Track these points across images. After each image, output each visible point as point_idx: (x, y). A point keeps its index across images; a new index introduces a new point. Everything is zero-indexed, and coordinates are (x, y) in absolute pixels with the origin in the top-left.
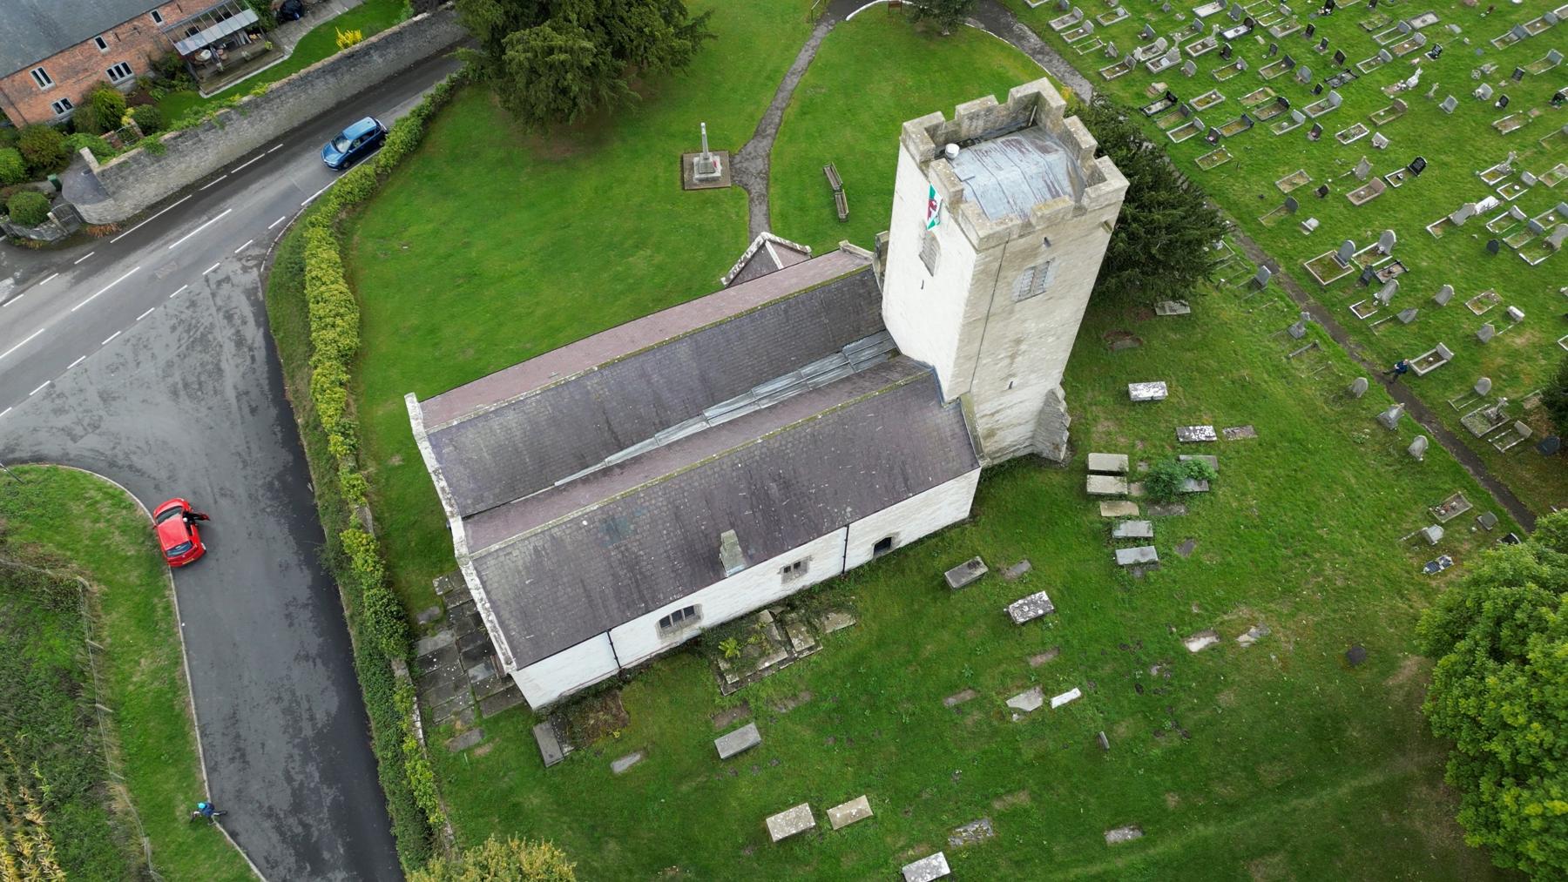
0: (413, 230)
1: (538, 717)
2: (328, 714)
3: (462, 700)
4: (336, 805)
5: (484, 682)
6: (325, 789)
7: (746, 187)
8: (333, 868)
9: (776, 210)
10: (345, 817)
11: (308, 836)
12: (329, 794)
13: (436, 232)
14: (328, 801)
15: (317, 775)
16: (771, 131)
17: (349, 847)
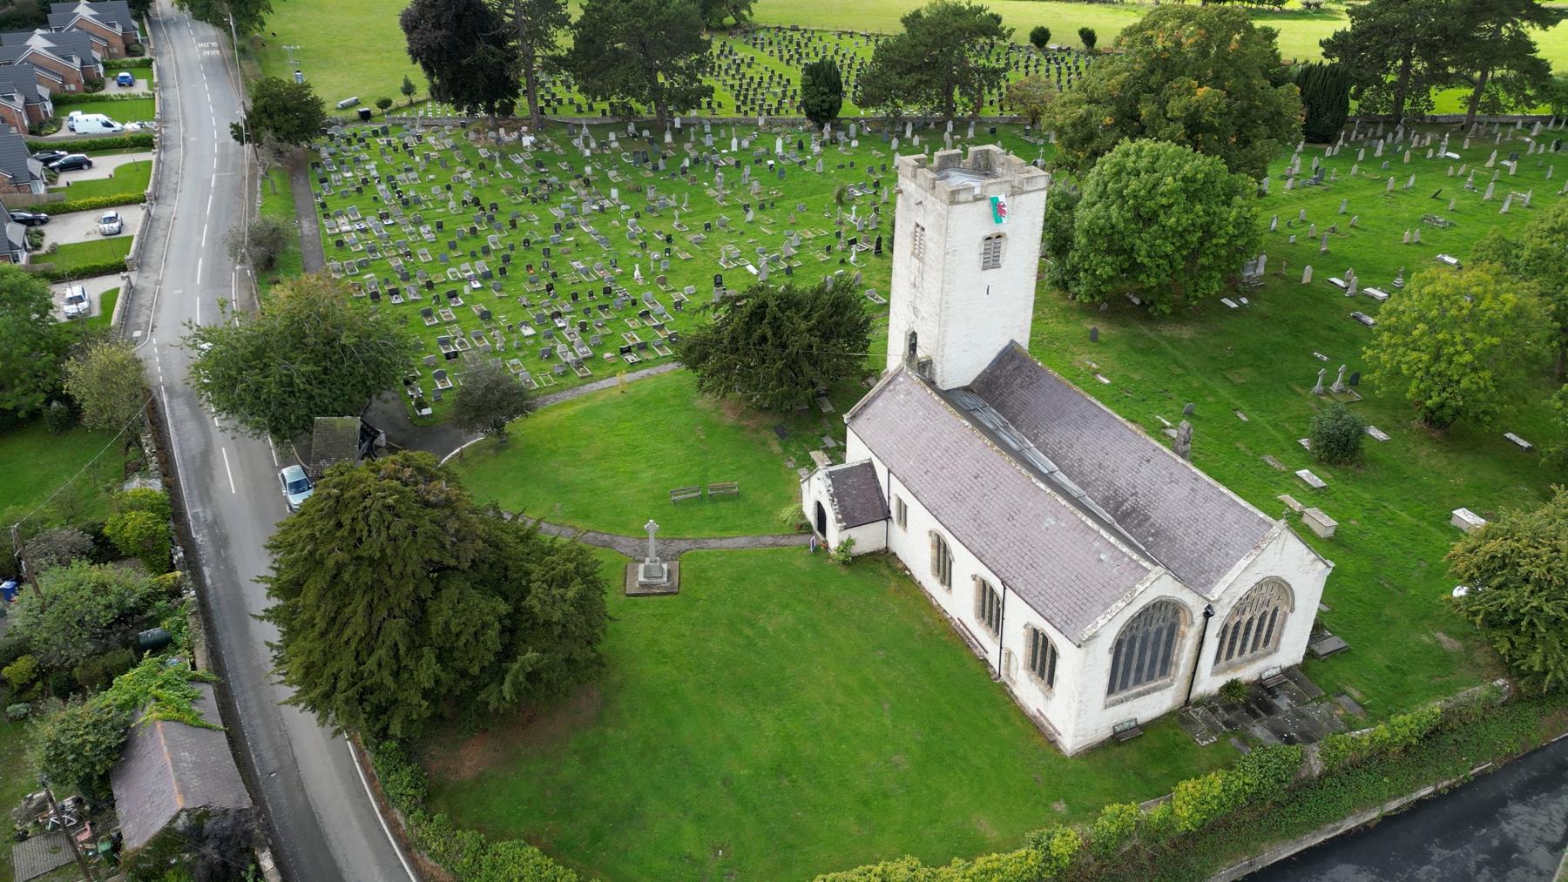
0: (689, 846)
1: (1310, 654)
2: (1359, 872)
3: (1317, 712)
4: (1448, 844)
5: (1291, 697)
6: (1435, 857)
7: (680, 553)
8: (1503, 835)
9: (717, 534)
10: (1453, 833)
11: (1488, 863)
12: (1439, 853)
13: (700, 818)
14: (1446, 853)
15: (1426, 868)
16: (606, 537)
17: (1478, 826)
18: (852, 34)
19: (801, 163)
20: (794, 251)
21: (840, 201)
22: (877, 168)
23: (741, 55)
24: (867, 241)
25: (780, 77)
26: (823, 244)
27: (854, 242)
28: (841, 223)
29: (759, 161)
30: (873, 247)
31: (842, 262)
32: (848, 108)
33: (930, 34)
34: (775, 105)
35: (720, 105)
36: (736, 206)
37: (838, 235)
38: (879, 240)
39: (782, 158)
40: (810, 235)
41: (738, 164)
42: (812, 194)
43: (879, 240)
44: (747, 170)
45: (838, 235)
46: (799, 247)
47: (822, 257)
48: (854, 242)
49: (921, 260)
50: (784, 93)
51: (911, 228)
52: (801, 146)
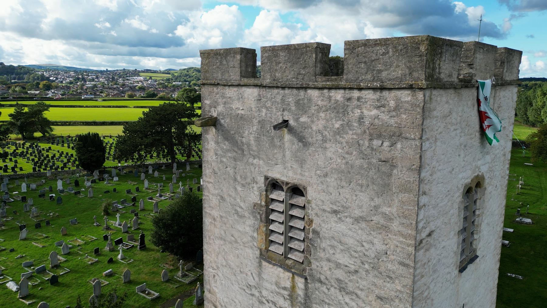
18: (111, 137)
19: (76, 193)
20: (62, 259)
21: (107, 213)
22: (133, 190)
23: (42, 147)
24: (131, 239)
25: (67, 154)
26: (91, 248)
27: (120, 242)
28: (108, 228)
29: (42, 195)
30: (137, 244)
31: (111, 261)
32: (109, 163)
33: (157, 114)
34: (61, 165)
35: (21, 169)
36: (13, 229)
37: (106, 238)
38: (143, 237)
39: (62, 191)
40: (80, 242)
41: (24, 199)
42: (84, 211)
43: (143, 237)
44: (30, 202)
45: (106, 238)
46: (69, 254)
47: (91, 259)
48: (120, 242)
49: (300, 270)
50: (69, 161)
51: (255, 195)
52: (77, 184)
